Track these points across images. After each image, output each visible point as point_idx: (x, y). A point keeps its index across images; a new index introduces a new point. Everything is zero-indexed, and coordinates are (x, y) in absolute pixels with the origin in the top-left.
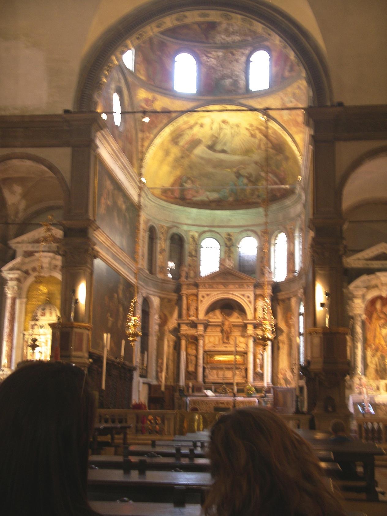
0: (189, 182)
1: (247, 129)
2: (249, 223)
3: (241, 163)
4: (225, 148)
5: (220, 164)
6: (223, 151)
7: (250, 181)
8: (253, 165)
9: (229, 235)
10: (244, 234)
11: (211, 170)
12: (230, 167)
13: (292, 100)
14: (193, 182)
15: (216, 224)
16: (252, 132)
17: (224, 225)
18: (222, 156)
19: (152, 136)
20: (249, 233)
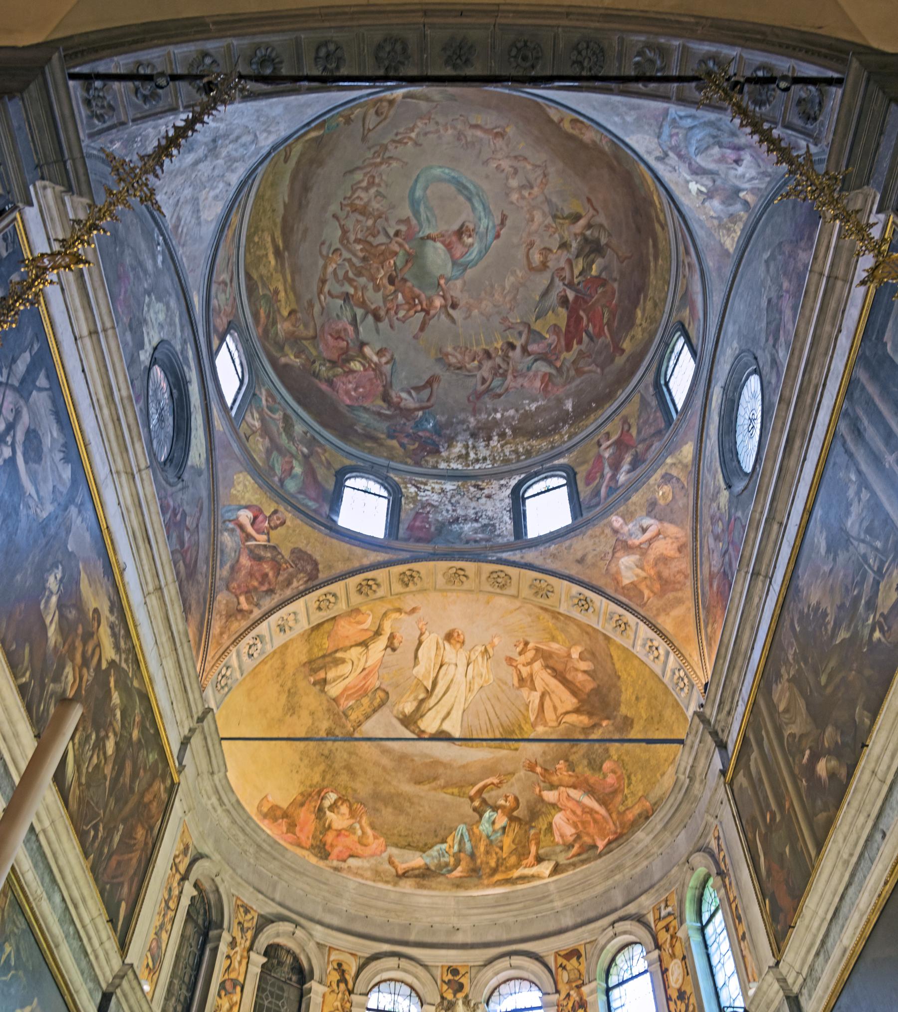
0: (344, 809)
1: (510, 660)
2: (517, 935)
3: (489, 770)
4: (447, 727)
5: (428, 774)
6: (442, 737)
7: (512, 819)
8: (522, 773)
9: (455, 971)
10: (505, 962)
11: (408, 788)
12: (461, 785)
13: (646, 522)
14: (353, 814)
15: (412, 938)
16: (525, 671)
17: (435, 940)
18: (439, 749)
19: (257, 613)
20: (516, 960)
